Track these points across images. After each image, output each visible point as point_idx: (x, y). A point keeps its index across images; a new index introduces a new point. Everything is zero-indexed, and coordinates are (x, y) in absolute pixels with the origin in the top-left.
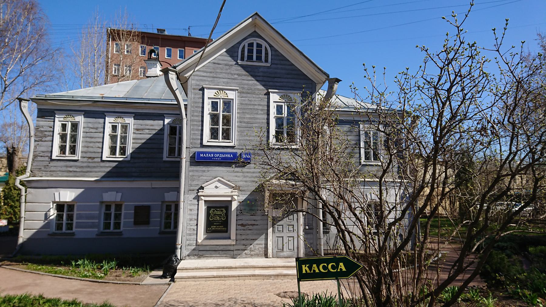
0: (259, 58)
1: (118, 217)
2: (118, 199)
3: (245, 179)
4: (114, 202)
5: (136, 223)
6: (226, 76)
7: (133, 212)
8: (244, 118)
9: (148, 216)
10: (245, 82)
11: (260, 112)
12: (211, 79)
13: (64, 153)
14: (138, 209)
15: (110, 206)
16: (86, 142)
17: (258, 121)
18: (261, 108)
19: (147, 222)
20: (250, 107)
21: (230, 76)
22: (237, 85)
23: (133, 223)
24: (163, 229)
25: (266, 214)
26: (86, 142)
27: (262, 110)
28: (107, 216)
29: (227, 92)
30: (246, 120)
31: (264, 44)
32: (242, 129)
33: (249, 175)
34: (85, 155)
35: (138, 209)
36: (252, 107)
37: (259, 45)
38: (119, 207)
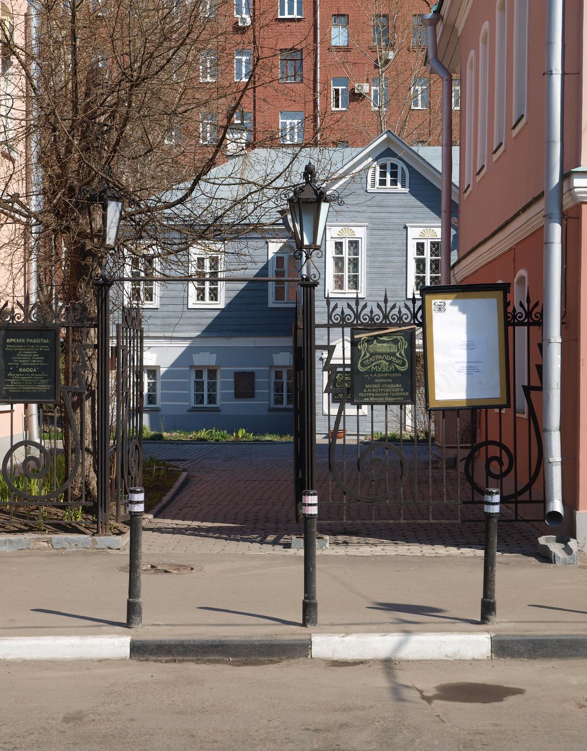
0: (394, 183)
1: (212, 386)
2: (213, 363)
4: (206, 366)
5: (238, 395)
7: (233, 380)
9: (252, 386)
10: (377, 215)
11: (395, 253)
14: (238, 376)
15: (201, 372)
17: (393, 264)
18: (396, 247)
19: (251, 395)
23: (233, 395)
24: (272, 405)
27: (398, 250)
28: (199, 385)
29: (351, 228)
30: (377, 264)
31: (400, 165)
32: (371, 276)
34: (165, 301)
35: (238, 376)
36: (385, 247)
37: (394, 166)
38: (212, 373)
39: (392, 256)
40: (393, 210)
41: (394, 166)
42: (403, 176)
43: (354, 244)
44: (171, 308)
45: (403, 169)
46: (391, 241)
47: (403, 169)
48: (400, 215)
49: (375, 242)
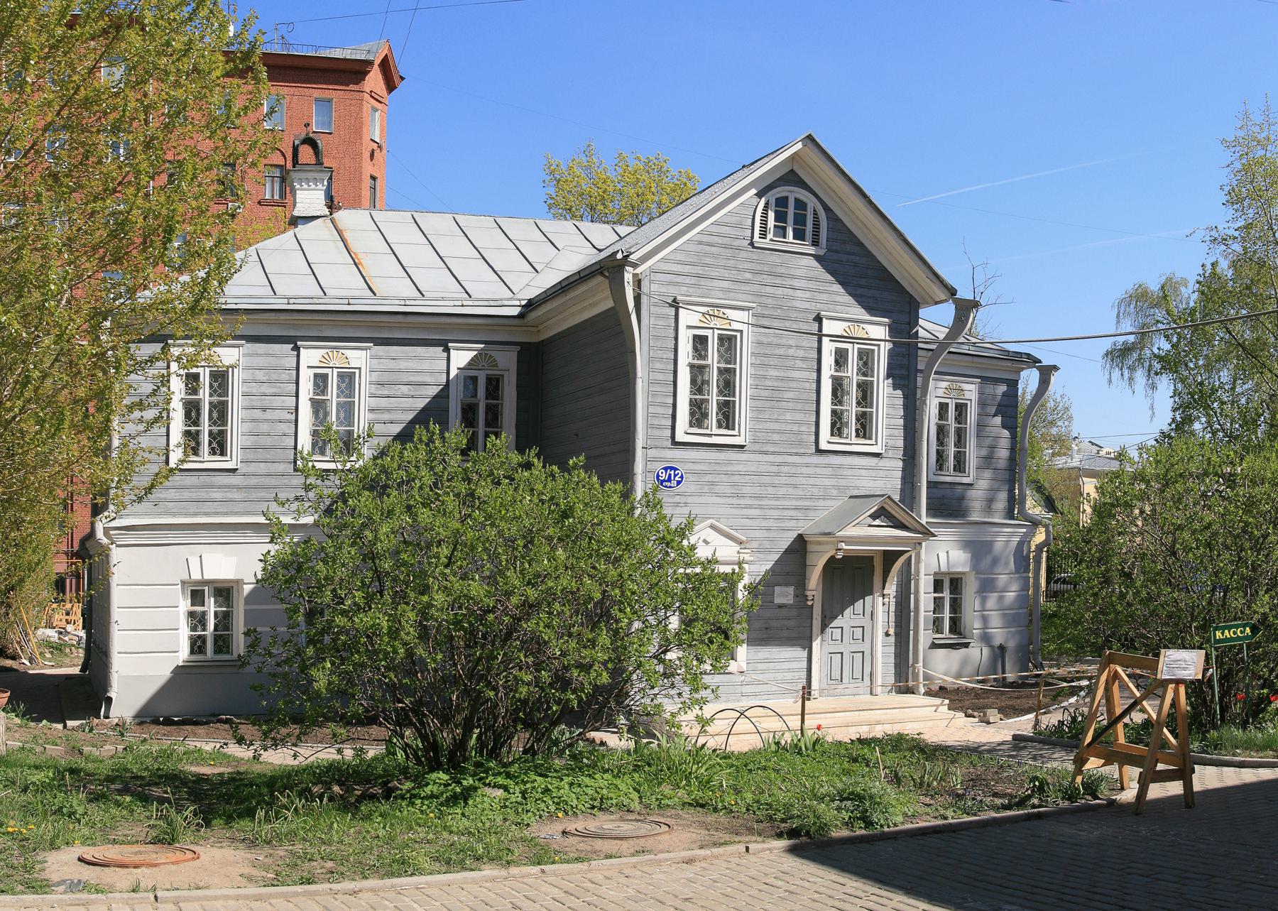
3: (765, 524)
6: (726, 274)
8: (765, 377)
11: (799, 364)
12: (693, 280)
13: (196, 451)
16: (253, 420)
17: (794, 385)
18: (801, 353)
20: (777, 352)
21: (734, 274)
22: (750, 298)
25: (810, 603)
26: (253, 420)
27: (804, 359)
30: (768, 383)
32: (759, 404)
33: (776, 513)
34: (251, 456)
36: (782, 351)
39: (793, 368)
40: (796, 283)
41: (800, 205)
42: (816, 226)
43: (728, 342)
44: (262, 468)
45: (815, 213)
46: (792, 342)
47: (815, 213)
48: (808, 295)
49: (765, 340)
